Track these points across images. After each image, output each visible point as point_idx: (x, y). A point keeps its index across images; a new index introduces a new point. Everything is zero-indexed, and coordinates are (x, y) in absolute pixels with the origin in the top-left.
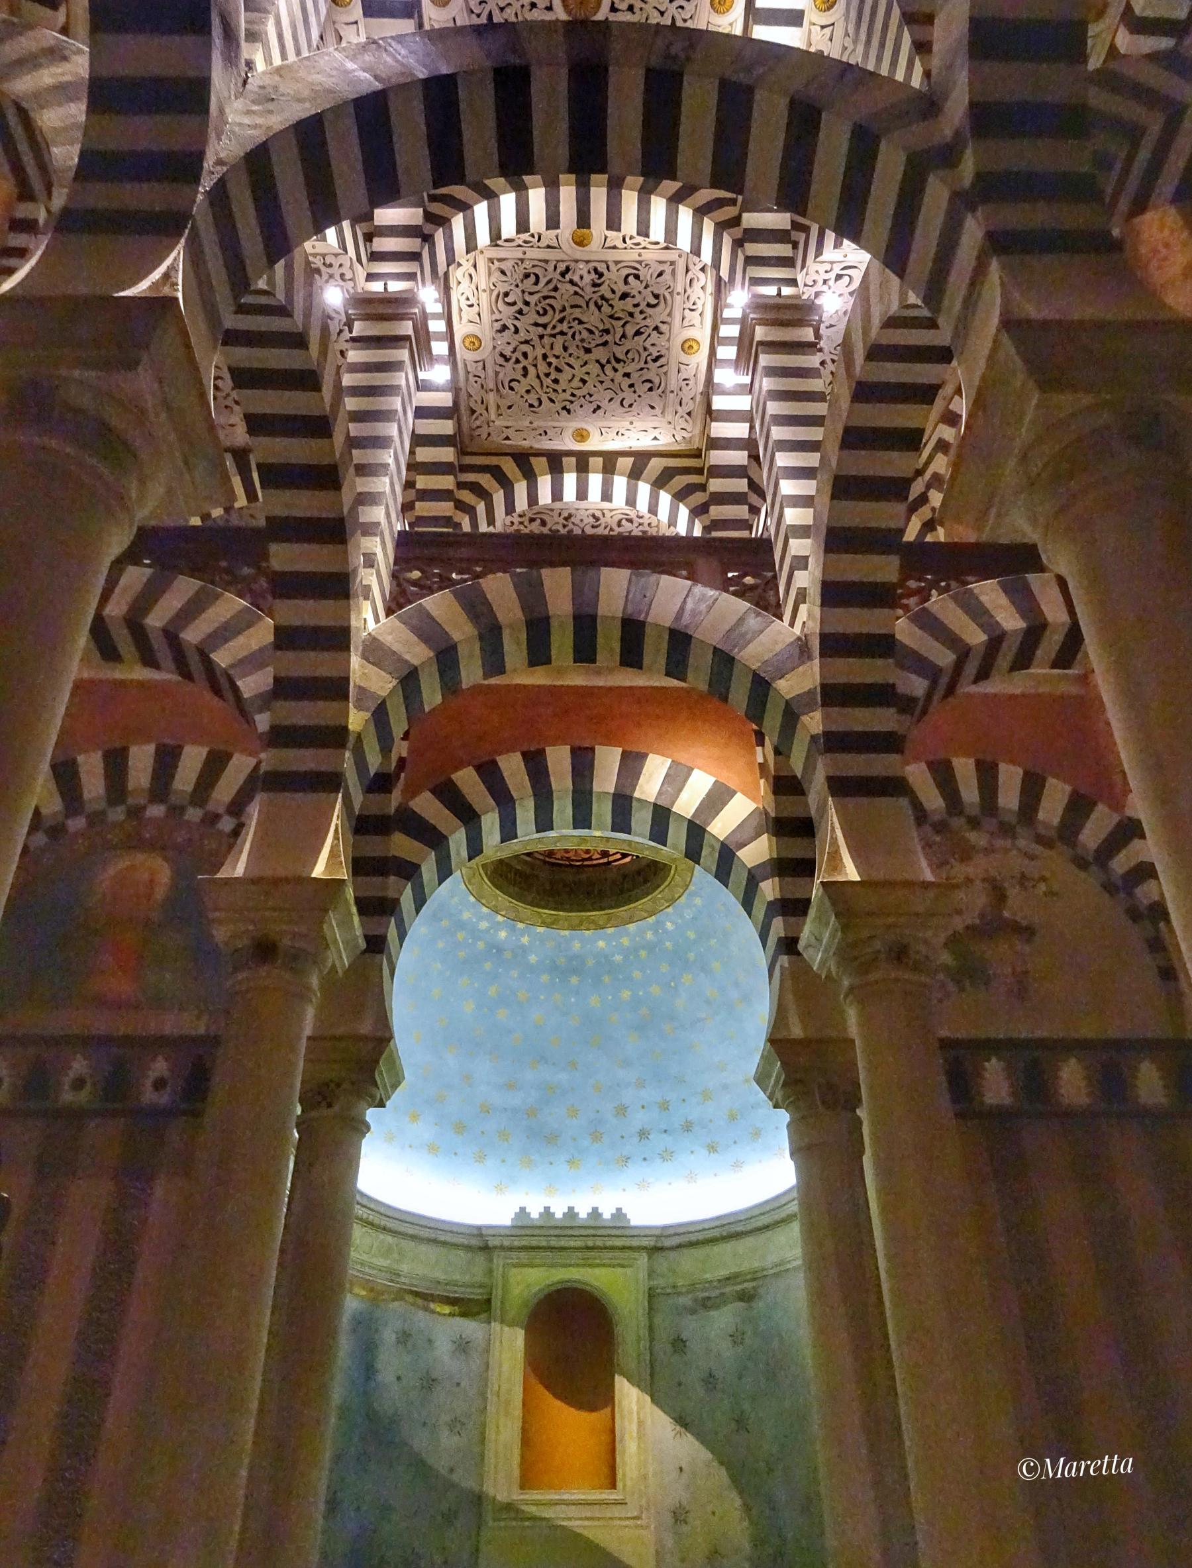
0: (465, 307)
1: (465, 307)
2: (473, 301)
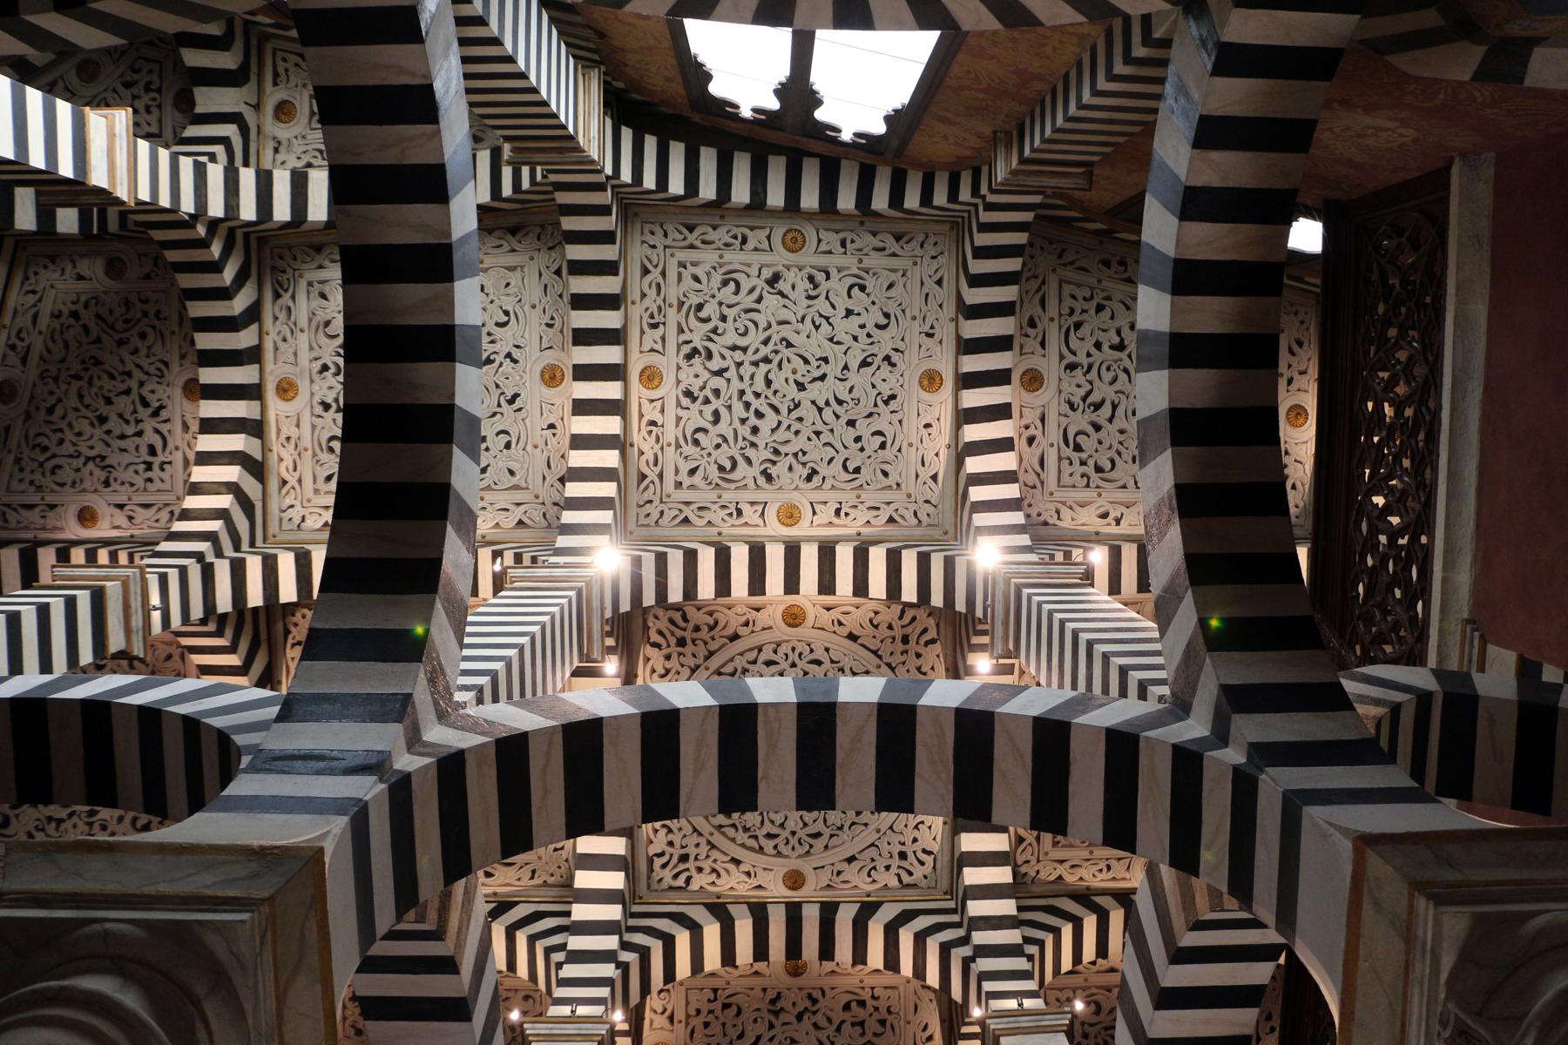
0: (1111, 874)
1: (1111, 874)
2: (1102, 865)
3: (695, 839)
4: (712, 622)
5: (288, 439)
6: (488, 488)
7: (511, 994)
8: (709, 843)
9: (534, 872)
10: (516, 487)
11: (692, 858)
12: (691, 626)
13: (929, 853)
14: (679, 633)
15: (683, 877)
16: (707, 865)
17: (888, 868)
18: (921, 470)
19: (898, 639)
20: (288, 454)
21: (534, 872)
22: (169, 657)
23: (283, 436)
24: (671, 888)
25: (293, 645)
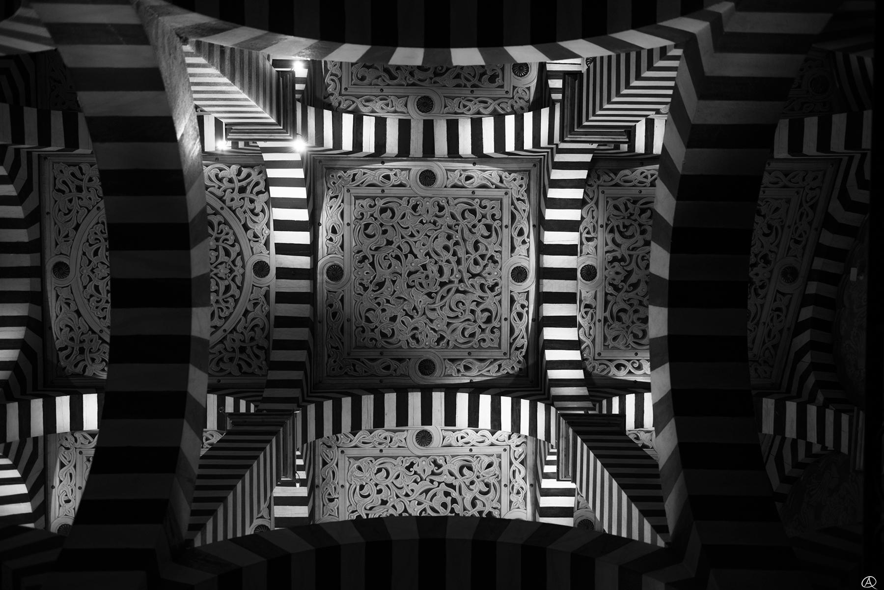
3: (234, 205)
4: (221, 365)
5: (518, 493)
6: (376, 458)
7: (375, 81)
8: (224, 202)
9: (353, 180)
10: (357, 459)
11: (236, 190)
12: (236, 362)
13: (59, 190)
14: (244, 356)
15: (243, 175)
16: (226, 184)
17: (90, 180)
18: (72, 471)
19: (87, 351)
20: (519, 482)
21: (353, 180)
22: (615, 339)
23: (522, 495)
24: (252, 167)
25: (522, 347)
